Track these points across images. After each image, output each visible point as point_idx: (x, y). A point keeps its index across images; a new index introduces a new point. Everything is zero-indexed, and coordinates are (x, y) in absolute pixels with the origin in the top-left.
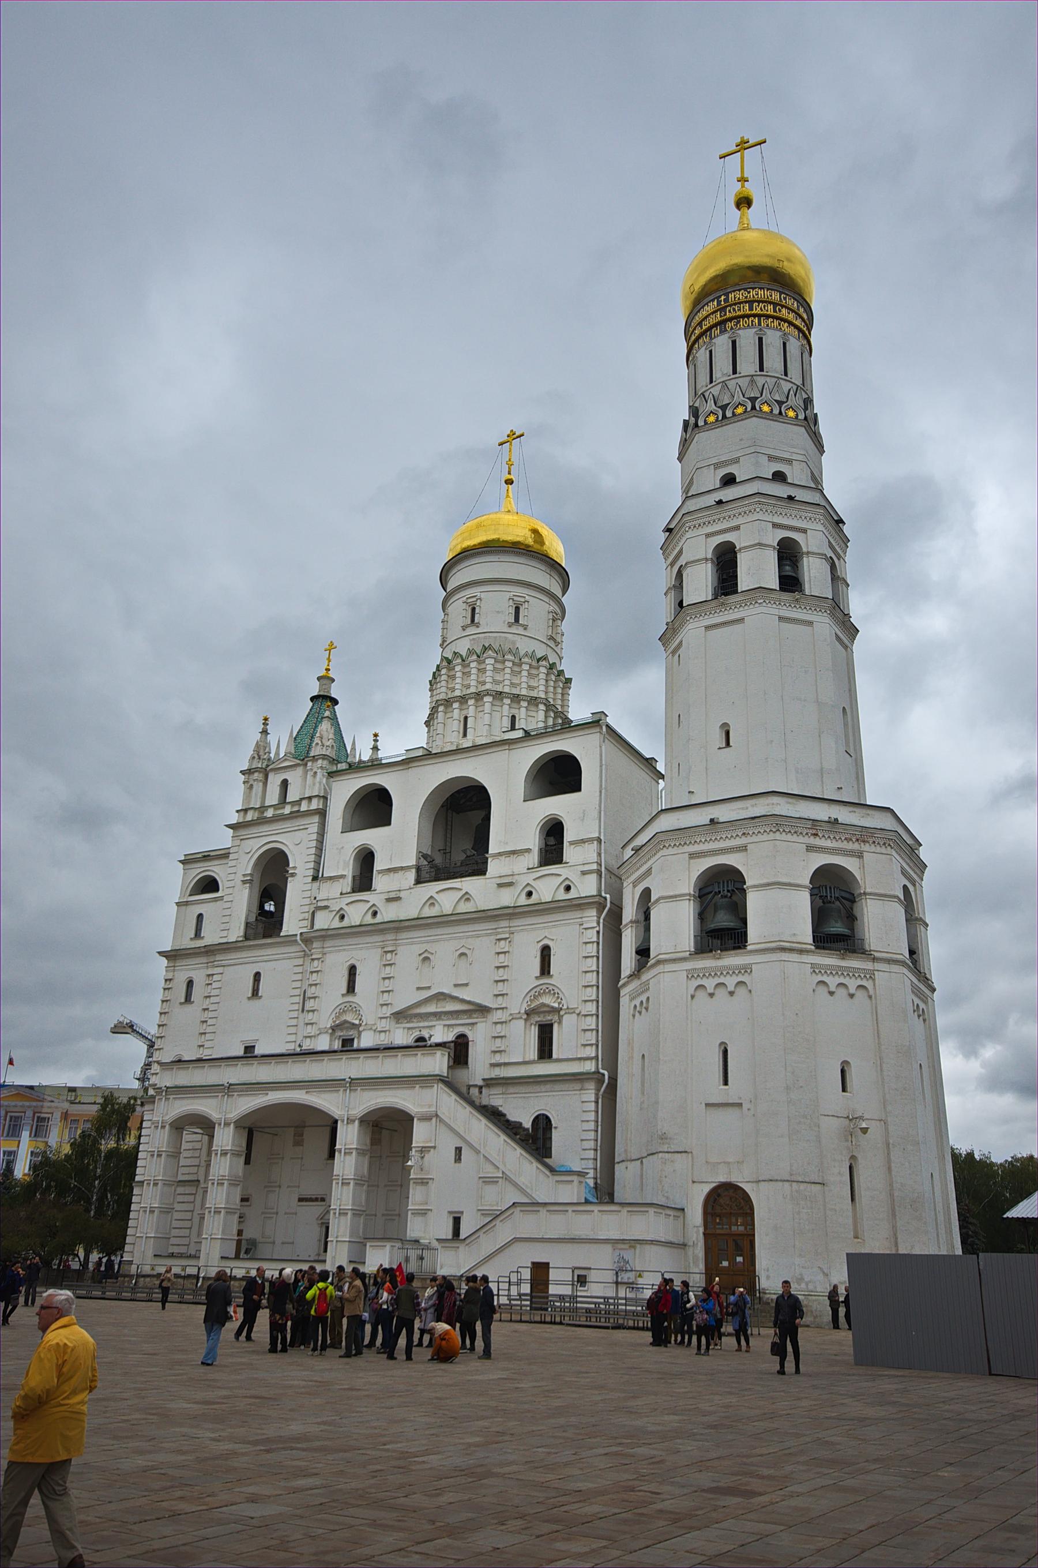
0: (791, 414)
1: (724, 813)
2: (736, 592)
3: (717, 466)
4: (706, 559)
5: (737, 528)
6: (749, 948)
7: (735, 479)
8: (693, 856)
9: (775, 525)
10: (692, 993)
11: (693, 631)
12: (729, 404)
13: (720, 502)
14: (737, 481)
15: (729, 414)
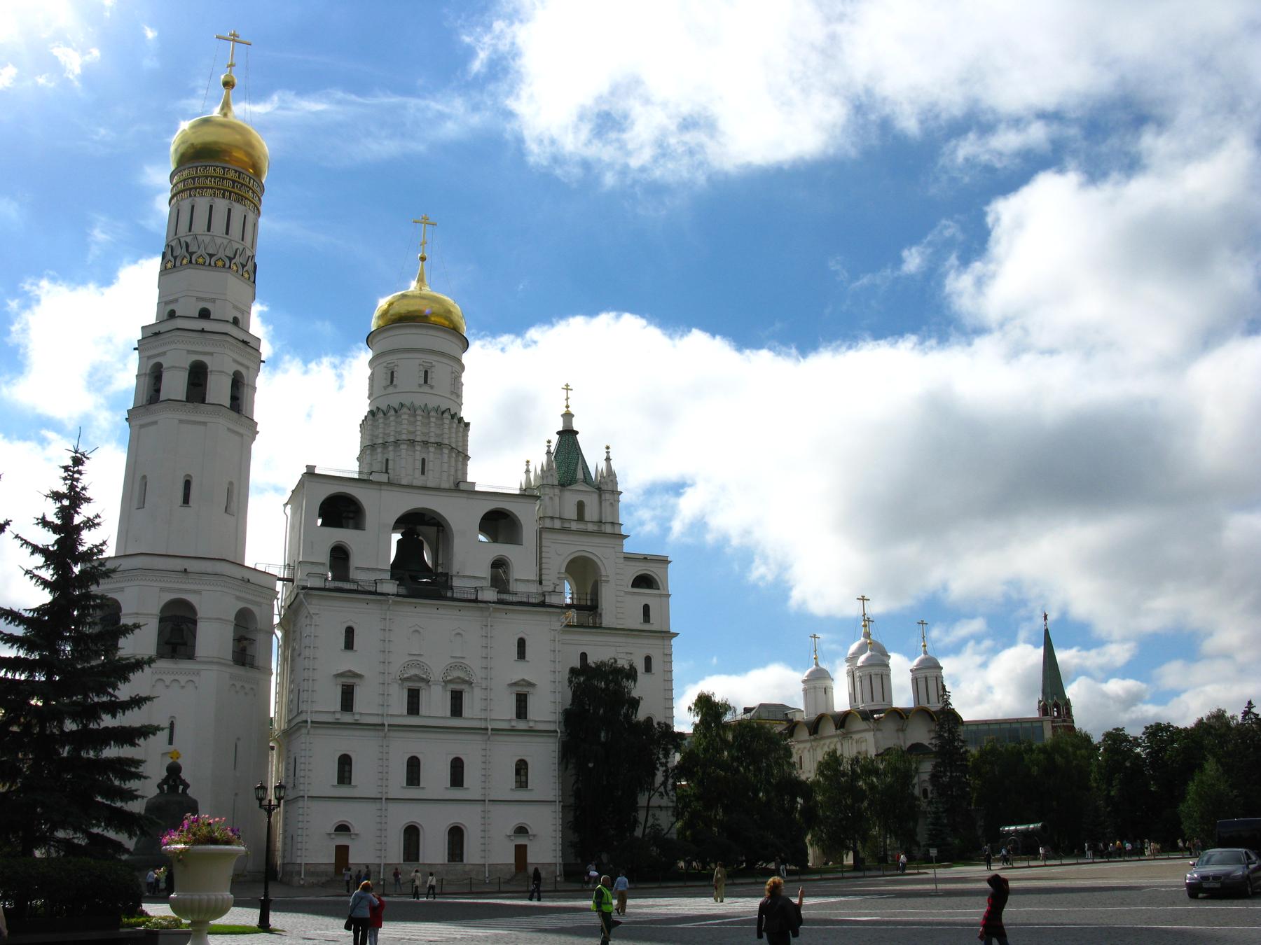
0: (246, 275)
1: (193, 566)
2: (203, 401)
3: (199, 299)
4: (185, 368)
5: (211, 354)
6: (198, 659)
7: (210, 314)
8: (162, 589)
9: (235, 361)
10: (154, 684)
11: (166, 418)
12: (214, 255)
13: (203, 331)
14: (211, 317)
15: (213, 264)
